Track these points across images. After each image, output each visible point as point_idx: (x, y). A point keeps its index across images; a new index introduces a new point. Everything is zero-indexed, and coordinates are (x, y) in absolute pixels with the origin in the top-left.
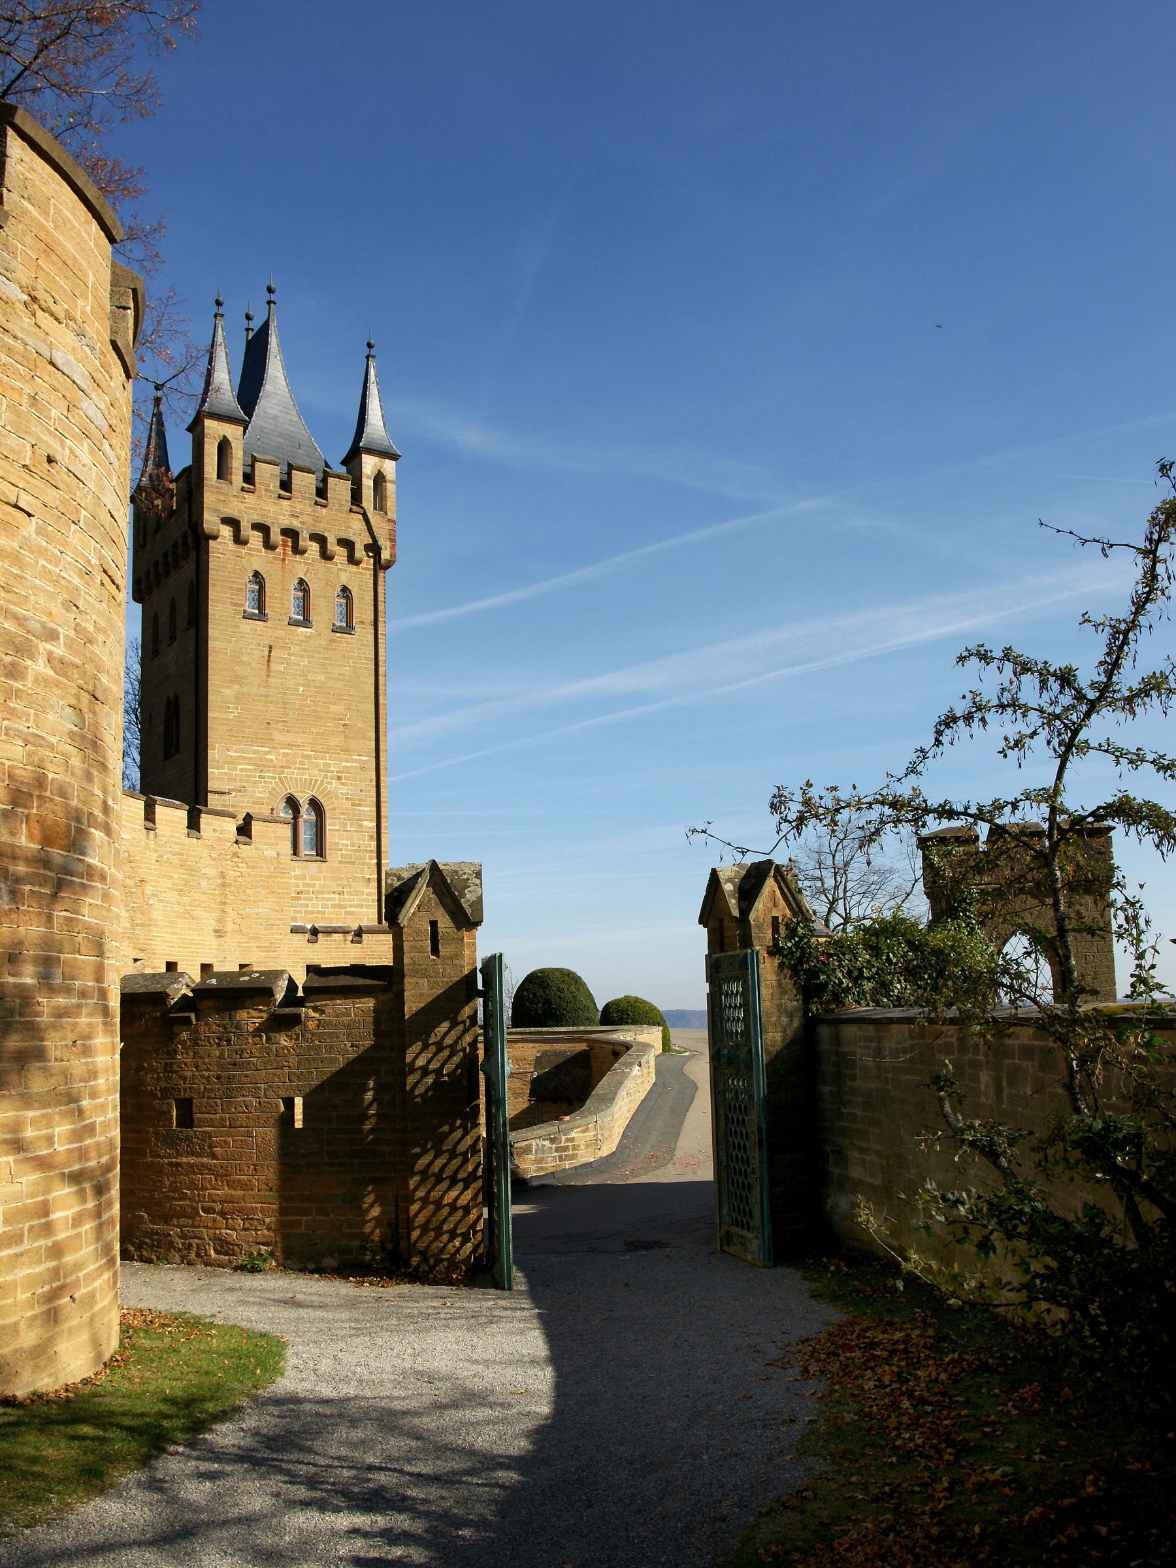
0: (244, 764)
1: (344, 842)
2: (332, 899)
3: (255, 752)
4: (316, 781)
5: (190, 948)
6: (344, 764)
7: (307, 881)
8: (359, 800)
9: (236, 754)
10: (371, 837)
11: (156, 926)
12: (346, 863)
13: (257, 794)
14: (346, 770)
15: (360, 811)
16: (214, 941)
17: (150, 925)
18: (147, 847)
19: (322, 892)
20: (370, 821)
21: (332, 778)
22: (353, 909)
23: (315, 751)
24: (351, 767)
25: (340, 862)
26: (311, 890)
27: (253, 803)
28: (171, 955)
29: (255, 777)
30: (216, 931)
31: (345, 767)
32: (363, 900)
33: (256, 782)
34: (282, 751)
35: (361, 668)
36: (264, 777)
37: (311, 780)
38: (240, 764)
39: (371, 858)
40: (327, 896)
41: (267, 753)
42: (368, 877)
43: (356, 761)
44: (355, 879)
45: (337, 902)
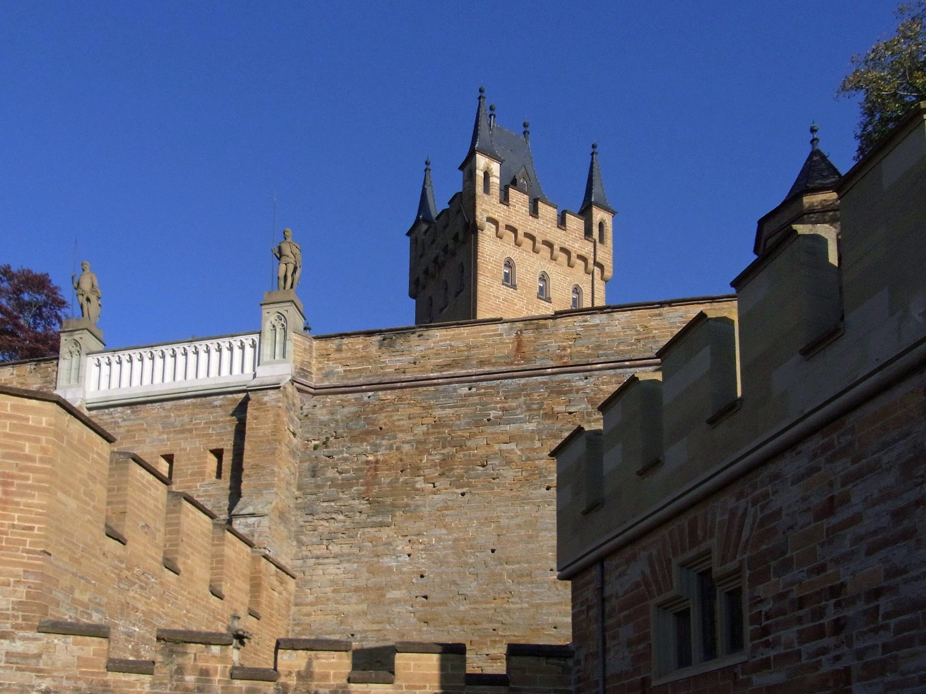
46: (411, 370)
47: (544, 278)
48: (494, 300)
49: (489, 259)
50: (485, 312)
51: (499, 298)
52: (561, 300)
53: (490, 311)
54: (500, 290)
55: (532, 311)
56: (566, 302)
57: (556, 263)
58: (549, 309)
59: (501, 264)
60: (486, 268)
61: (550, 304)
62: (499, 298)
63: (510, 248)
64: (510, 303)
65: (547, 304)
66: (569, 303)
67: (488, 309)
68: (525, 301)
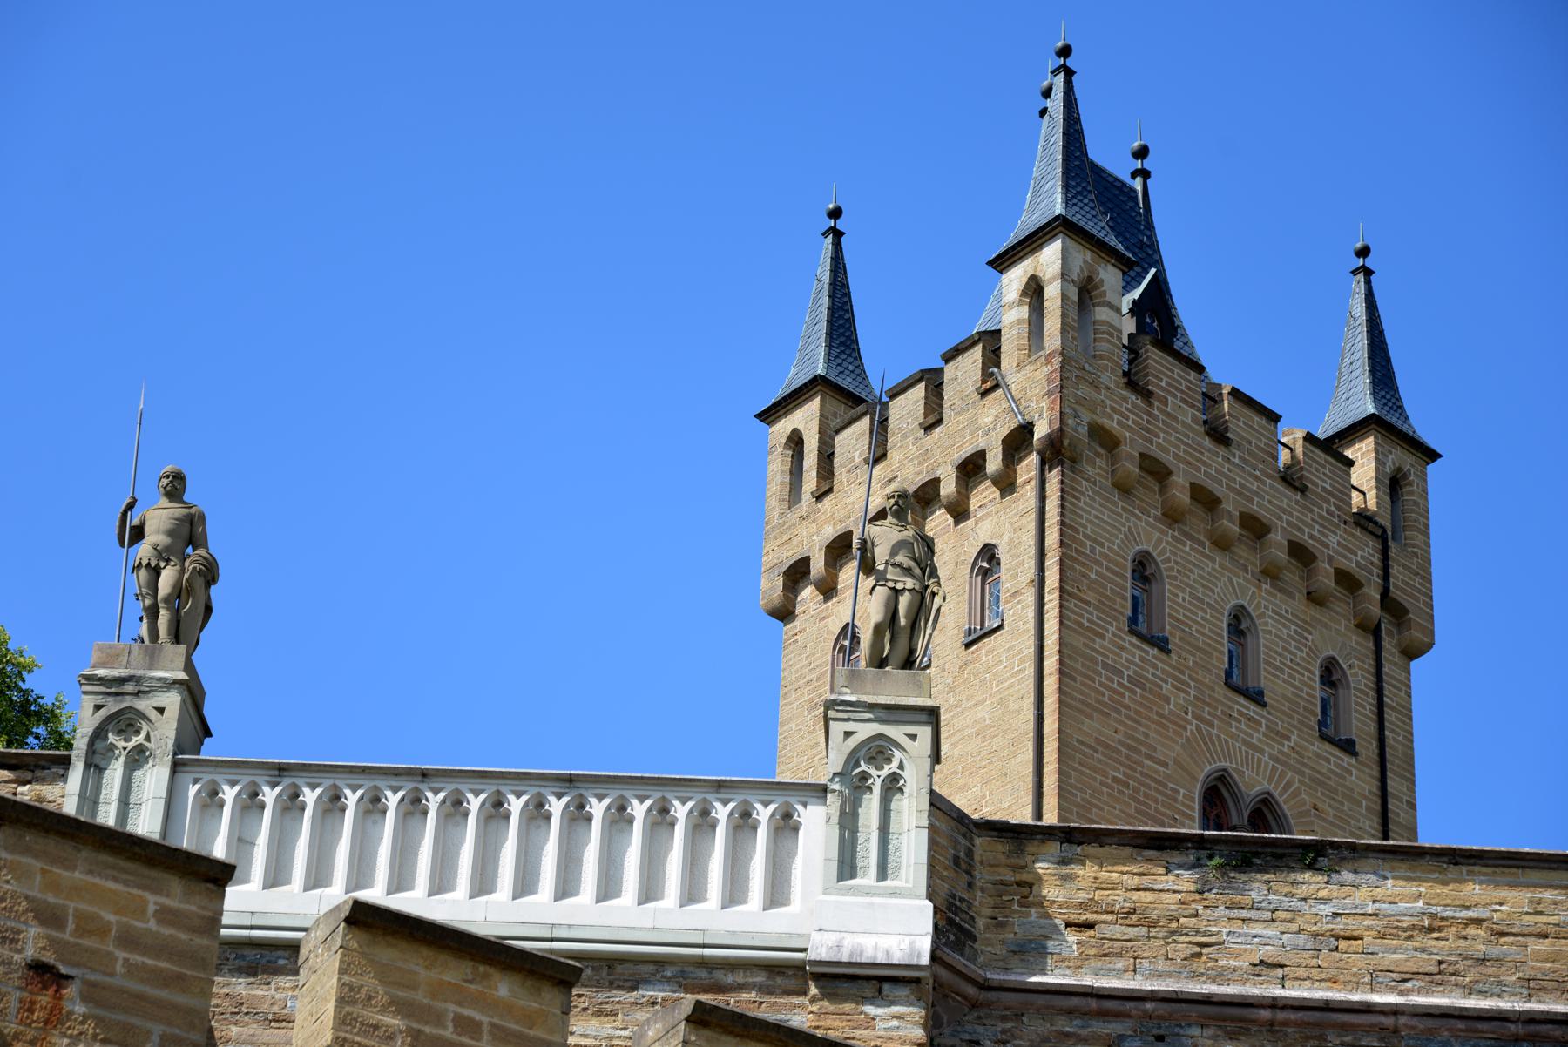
46: (1301, 972)
47: (1239, 625)
48: (1107, 678)
49: (1093, 550)
50: (1082, 712)
51: (1120, 674)
52: (1289, 700)
53: (1096, 710)
54: (1122, 648)
55: (1212, 726)
56: (1305, 708)
57: (1272, 586)
58: (1260, 724)
59: (1124, 567)
60: (1084, 575)
61: (1259, 709)
62: (1120, 674)
63: (1147, 523)
65: (1252, 707)
66: (1316, 715)
67: (1088, 705)
68: (1192, 692)
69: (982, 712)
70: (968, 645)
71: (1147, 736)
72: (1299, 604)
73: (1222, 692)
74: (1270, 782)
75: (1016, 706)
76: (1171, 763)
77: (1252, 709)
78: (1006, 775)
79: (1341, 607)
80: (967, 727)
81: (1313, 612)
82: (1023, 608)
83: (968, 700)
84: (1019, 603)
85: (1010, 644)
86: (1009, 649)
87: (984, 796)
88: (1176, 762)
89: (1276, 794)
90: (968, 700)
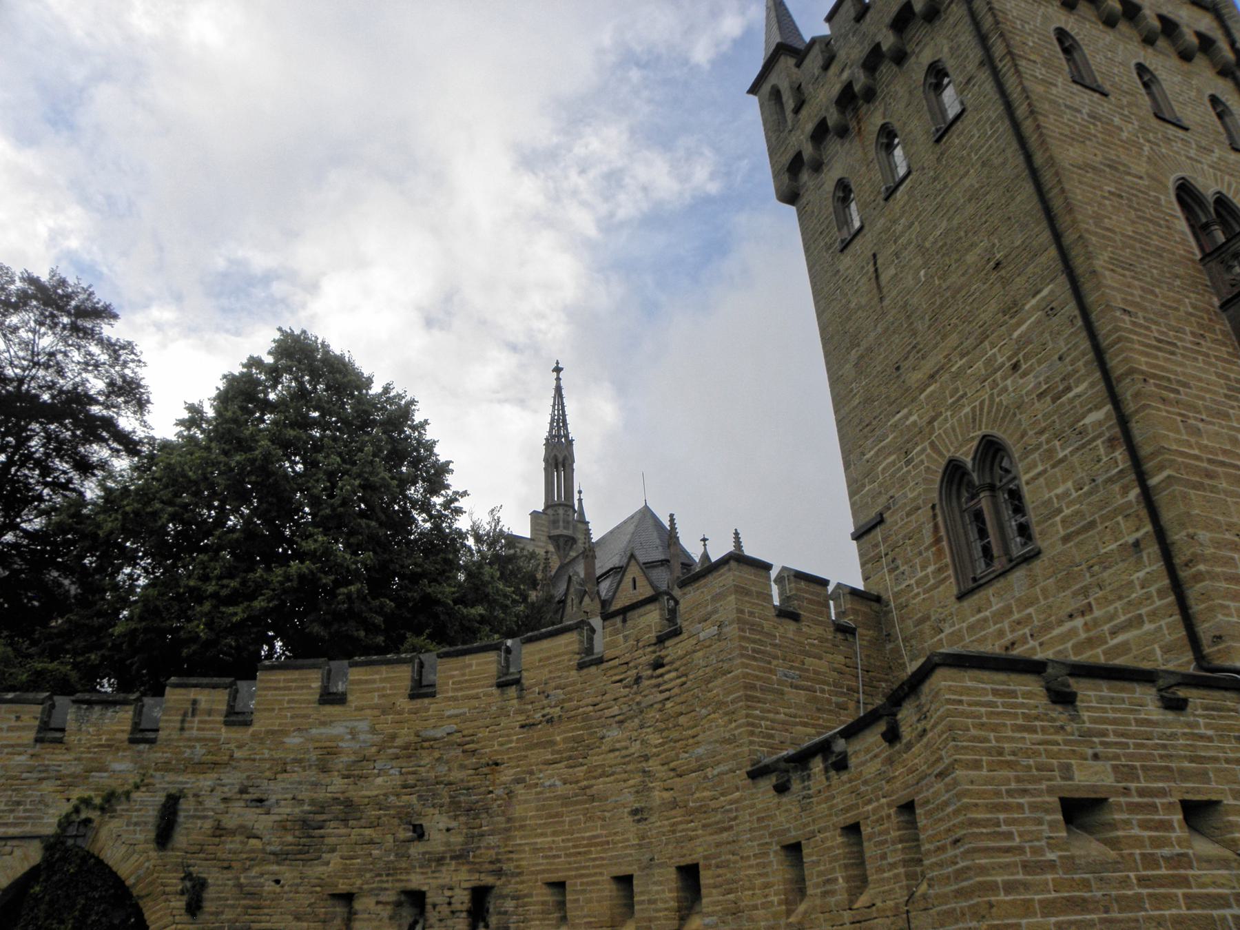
0: (885, 458)
1: (1059, 491)
2: (1073, 632)
3: (895, 426)
4: (982, 403)
5: (590, 852)
6: (1016, 335)
7: (1016, 616)
8: (1063, 379)
9: (872, 453)
10: (1111, 443)
11: (522, 827)
12: (1078, 533)
13: (911, 496)
14: (1024, 341)
15: (1071, 401)
16: (628, 828)
17: (508, 830)
18: (503, 712)
19: (1047, 627)
20: (1097, 407)
21: (1004, 378)
22: (1121, 638)
23: (968, 353)
24: (1028, 329)
25: (1066, 539)
26: (1027, 631)
27: (908, 515)
28: (557, 870)
29: (901, 468)
30: (635, 812)
31: (1020, 336)
32: (1140, 603)
33: (903, 479)
34: (923, 396)
35: (990, 147)
36: (912, 459)
37: (973, 409)
38: (880, 463)
39: (1125, 490)
40: (1056, 632)
41: (906, 417)
42: (1131, 539)
43: (1036, 308)
44: (1105, 562)
45: (1083, 636)
49: (1023, 26)
64: (1107, 124)
69: (971, 181)
70: (938, 141)
71: (1119, 157)
72: (1175, 61)
73: (1155, 123)
74: (1217, 184)
75: (1000, 160)
76: (1145, 177)
77: (1181, 133)
78: (1009, 218)
79: (1201, 62)
80: (959, 199)
81: (1186, 66)
82: (980, 86)
83: (952, 179)
84: (974, 85)
85: (977, 118)
86: (978, 123)
87: (994, 245)
88: (1149, 176)
89: (1225, 192)
90: (952, 179)
